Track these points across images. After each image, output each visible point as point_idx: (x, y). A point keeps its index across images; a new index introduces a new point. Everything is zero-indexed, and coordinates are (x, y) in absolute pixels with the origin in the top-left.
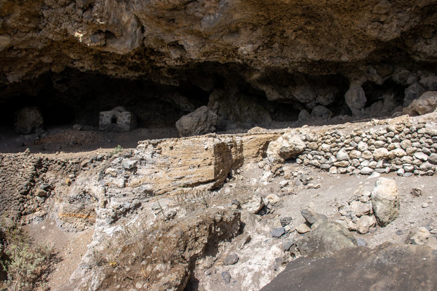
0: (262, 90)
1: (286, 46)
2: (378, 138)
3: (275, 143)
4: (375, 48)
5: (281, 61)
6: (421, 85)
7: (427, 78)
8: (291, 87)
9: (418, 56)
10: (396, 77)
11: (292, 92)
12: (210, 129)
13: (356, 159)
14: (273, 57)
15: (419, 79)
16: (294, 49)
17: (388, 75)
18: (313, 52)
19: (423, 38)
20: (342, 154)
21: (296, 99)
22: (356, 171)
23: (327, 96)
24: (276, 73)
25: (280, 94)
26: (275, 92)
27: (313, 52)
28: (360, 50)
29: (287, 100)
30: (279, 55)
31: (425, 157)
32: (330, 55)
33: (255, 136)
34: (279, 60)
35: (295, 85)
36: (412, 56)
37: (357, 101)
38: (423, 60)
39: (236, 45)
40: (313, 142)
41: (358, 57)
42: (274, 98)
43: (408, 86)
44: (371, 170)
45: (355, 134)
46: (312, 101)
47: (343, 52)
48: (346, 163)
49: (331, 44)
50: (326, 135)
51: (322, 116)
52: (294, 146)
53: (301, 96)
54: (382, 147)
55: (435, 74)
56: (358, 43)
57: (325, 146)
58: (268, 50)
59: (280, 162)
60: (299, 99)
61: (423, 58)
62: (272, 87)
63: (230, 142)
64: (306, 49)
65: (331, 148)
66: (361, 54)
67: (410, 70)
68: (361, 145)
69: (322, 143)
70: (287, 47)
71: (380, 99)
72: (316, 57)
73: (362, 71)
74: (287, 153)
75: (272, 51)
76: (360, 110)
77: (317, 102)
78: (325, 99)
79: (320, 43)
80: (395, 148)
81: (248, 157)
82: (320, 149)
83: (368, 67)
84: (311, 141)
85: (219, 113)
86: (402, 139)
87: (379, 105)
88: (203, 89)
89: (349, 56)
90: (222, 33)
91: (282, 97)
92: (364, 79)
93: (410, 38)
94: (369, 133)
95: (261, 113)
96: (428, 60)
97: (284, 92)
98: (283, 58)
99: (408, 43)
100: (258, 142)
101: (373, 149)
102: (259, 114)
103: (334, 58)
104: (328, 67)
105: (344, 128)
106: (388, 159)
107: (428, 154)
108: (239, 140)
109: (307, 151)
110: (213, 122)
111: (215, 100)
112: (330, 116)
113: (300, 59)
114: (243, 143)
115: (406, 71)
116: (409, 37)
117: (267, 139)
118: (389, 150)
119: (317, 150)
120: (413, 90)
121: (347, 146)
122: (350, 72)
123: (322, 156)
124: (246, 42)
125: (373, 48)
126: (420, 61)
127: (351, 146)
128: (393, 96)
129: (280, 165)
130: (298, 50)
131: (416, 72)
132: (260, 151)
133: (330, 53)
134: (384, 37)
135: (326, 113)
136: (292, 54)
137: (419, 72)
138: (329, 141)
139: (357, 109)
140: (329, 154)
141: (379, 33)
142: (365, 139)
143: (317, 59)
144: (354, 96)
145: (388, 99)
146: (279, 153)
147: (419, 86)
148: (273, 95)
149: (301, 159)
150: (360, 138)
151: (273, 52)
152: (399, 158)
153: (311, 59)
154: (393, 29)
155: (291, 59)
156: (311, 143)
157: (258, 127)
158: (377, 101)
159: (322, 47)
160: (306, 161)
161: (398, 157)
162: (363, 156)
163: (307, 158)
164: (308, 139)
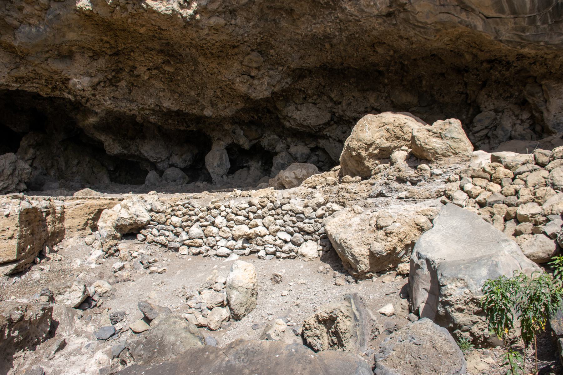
0: (99, 140)
1: (136, 86)
2: (239, 212)
3: (110, 212)
4: (244, 105)
5: (128, 105)
6: (290, 154)
7: (296, 147)
8: (138, 140)
9: (289, 121)
10: (265, 143)
11: (140, 146)
12: (19, 187)
13: (212, 238)
14: (117, 99)
15: (288, 147)
16: (146, 92)
17: (256, 139)
18: (170, 99)
19: (294, 102)
20: (195, 230)
21: (144, 156)
22: (212, 252)
23: (184, 157)
24: (120, 119)
25: (123, 148)
26: (117, 145)
27: (170, 99)
28: (227, 104)
29: (132, 156)
30: (126, 96)
31: (288, 238)
32: (191, 106)
33: (83, 200)
34: (125, 103)
35: (144, 138)
36: (282, 121)
37: (219, 166)
38: (293, 127)
39: (66, 75)
40: (160, 214)
41: (223, 114)
42: (115, 153)
43: (276, 154)
44: (228, 251)
45: (213, 206)
46: (164, 160)
47: (206, 105)
48: (200, 241)
49: (193, 93)
50: (177, 205)
51: (175, 181)
52: (135, 217)
53: (151, 153)
54: (242, 223)
55: (304, 144)
56: (225, 96)
57: (175, 219)
58: (112, 89)
59: (115, 237)
60: (148, 157)
62: (113, 137)
63: (46, 207)
64: (161, 94)
65: (183, 222)
66: (228, 110)
67: (280, 136)
68: (219, 220)
69: (172, 216)
70: (137, 88)
71: (246, 167)
72: (173, 106)
73: (227, 130)
74: (126, 226)
75: (117, 90)
76: (222, 177)
77: (170, 163)
78: (181, 160)
79: (179, 89)
80: (257, 226)
81: (71, 230)
82: (168, 223)
83: (234, 127)
84: (158, 212)
85: (34, 165)
86: (265, 215)
87: (244, 172)
88: (13, 129)
89: (213, 110)
90: (47, 55)
91: (125, 152)
92: (228, 141)
93: (281, 100)
94: (229, 206)
95: (95, 170)
96: (298, 128)
97: (129, 145)
98: (132, 101)
99: (279, 105)
100: (87, 210)
101: (232, 225)
102: (93, 172)
103: (195, 111)
104: (187, 120)
105: (200, 198)
106: (248, 239)
107: (291, 234)
108: (60, 205)
109: (152, 224)
110: (23, 177)
111: (30, 146)
112: (186, 182)
113: (153, 106)
114: (65, 210)
115: (276, 137)
116: (280, 99)
117: (100, 206)
118: (250, 228)
119: (164, 223)
120: (282, 159)
121: (202, 220)
122: (213, 130)
123: (171, 232)
124: (81, 73)
125: (241, 105)
126: (291, 127)
127: (206, 220)
128: (260, 164)
129: (115, 241)
130: (151, 93)
131: (286, 139)
132: (89, 222)
133: (191, 104)
134: (254, 95)
135: (180, 178)
136: (143, 98)
137: (289, 140)
138: (180, 213)
139: (218, 175)
140: (179, 230)
141: (249, 89)
142: (224, 213)
143: (175, 108)
144: (216, 160)
145: (255, 166)
146: (115, 225)
147: (288, 155)
148: (113, 147)
149: (144, 235)
150: (217, 212)
151: (118, 92)
152: (260, 238)
153: (166, 108)
154: (264, 87)
155: (142, 104)
156: (157, 215)
157: (89, 189)
158: (242, 168)
159: (181, 94)
160: (150, 238)
161: (259, 236)
162: (221, 233)
163: (151, 234)
164: (154, 209)
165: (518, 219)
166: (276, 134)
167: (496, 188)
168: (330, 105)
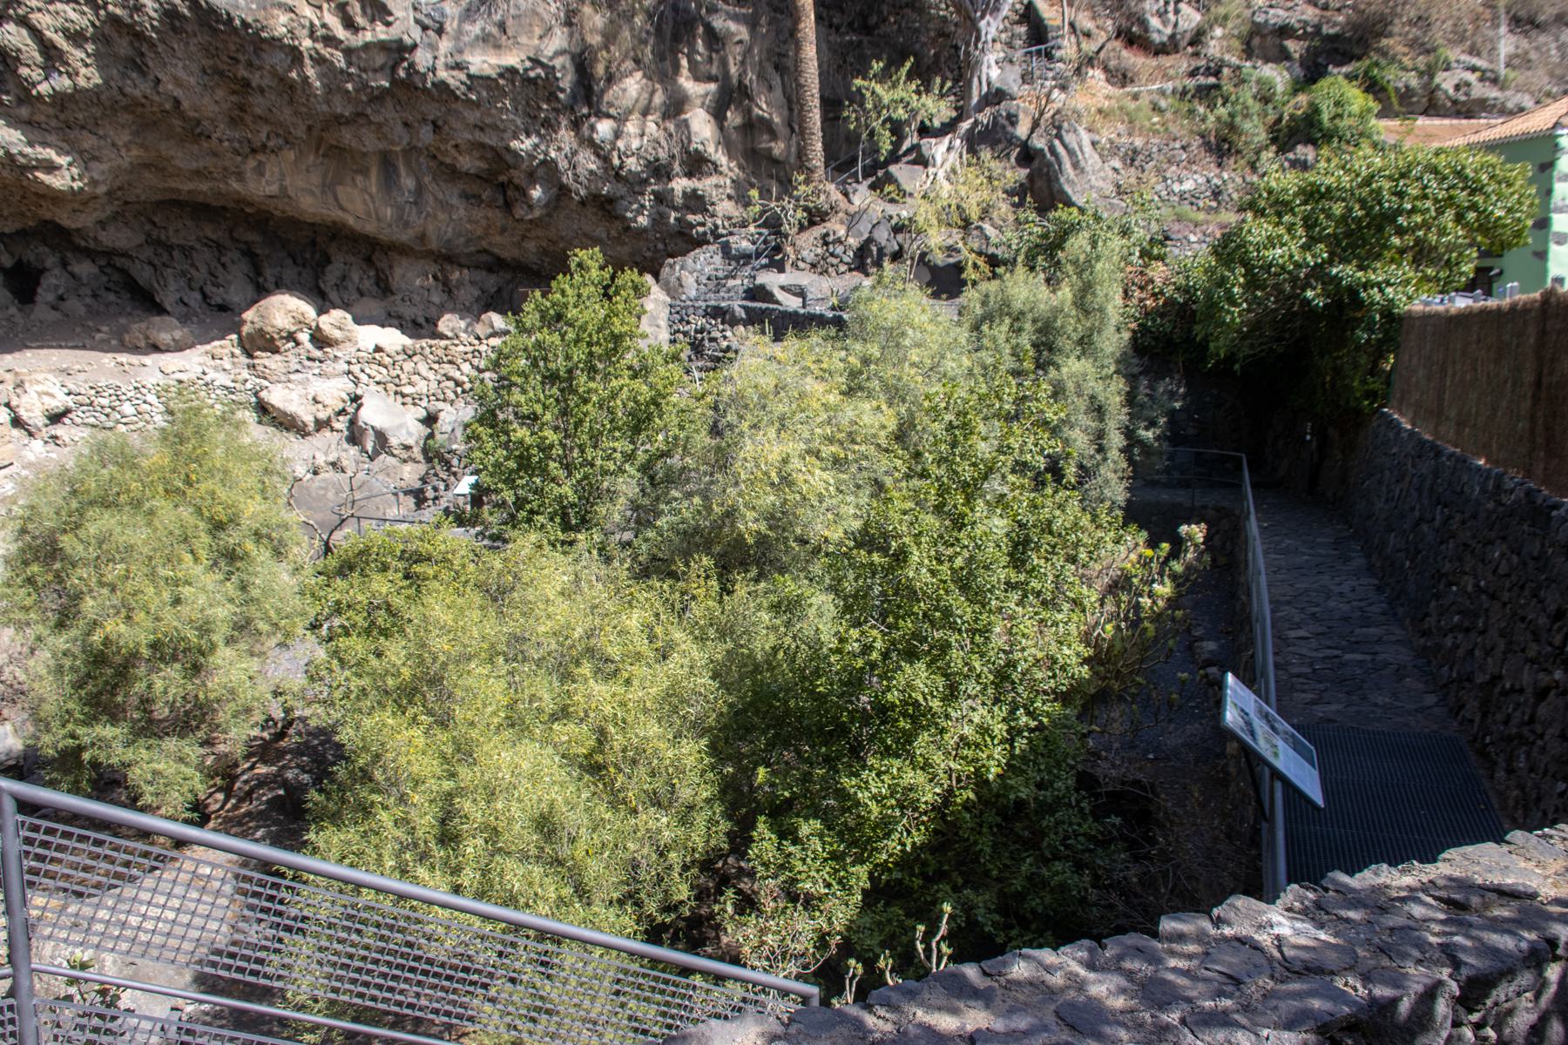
6: (73, 275)
10: (29, 256)
15: (64, 264)
43: (42, 271)
61: (92, 245)
67: (52, 247)
68: (151, 398)
137: (69, 255)
140: (108, 410)
165: (404, 396)
166: (46, 244)
167: (384, 371)
168: (148, 227)
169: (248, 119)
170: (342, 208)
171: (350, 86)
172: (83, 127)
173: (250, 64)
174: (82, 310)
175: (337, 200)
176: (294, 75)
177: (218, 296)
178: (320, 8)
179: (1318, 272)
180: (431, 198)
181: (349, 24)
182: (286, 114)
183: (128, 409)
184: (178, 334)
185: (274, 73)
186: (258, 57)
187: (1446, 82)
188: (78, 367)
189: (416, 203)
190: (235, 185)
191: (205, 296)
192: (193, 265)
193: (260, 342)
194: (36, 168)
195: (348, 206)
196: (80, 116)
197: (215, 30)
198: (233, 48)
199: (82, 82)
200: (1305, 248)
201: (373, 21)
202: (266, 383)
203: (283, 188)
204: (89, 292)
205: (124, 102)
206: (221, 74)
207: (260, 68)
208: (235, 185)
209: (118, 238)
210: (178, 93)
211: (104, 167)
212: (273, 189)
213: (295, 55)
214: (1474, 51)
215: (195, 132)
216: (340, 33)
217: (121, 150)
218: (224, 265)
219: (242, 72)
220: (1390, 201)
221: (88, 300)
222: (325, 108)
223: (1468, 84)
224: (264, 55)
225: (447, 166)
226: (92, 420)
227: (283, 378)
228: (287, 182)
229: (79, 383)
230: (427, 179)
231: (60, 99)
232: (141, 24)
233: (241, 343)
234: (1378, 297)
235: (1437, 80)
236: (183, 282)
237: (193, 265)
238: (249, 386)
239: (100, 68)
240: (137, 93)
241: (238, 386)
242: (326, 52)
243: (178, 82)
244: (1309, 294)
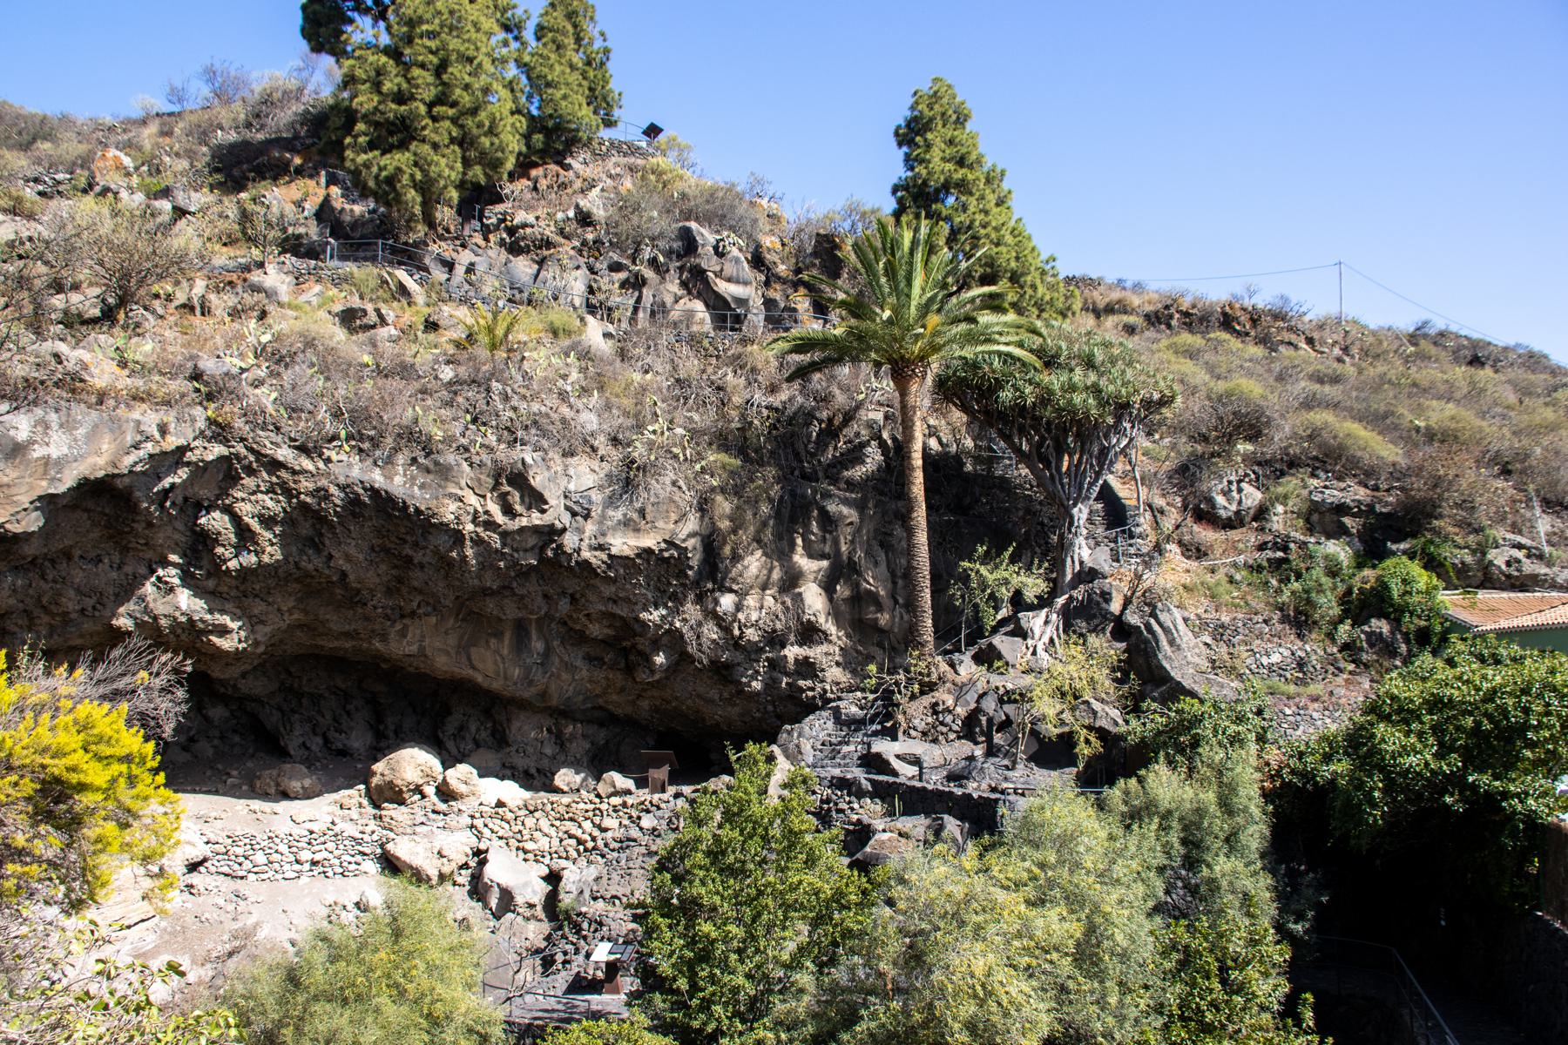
20: (260, 858)
22: (279, 876)
68: (283, 848)
165: (526, 852)
167: (506, 826)
169: (404, 590)
170: (474, 668)
171: (502, 564)
172: (256, 596)
173: (416, 545)
174: (210, 752)
175: (469, 659)
176: (454, 554)
177: (339, 741)
178: (484, 497)
179: (1456, 781)
180: (557, 660)
181: (508, 511)
182: (440, 587)
183: (260, 858)
184: (307, 782)
185: (436, 552)
186: (425, 539)
187: (1498, 558)
188: (214, 814)
189: (542, 664)
190: (378, 645)
191: (326, 741)
192: (319, 712)
193: (388, 794)
194: (211, 632)
195: (480, 666)
196: (257, 587)
197: (390, 516)
198: (403, 530)
199: (266, 559)
200: (1439, 756)
201: (529, 508)
202: (392, 835)
203: (422, 649)
204: (217, 734)
205: (298, 574)
206: (387, 551)
207: (424, 548)
208: (378, 645)
209: (257, 686)
210: (347, 567)
211: (268, 629)
212: (414, 649)
213: (458, 537)
214: (1515, 529)
215: (353, 599)
216: (499, 518)
217: (284, 613)
218: (348, 713)
219: (408, 551)
220: (1515, 717)
221: (216, 742)
222: (476, 582)
223: (1518, 561)
224: (430, 537)
225: (576, 632)
226: (226, 869)
227: (409, 830)
228: (426, 643)
229: (216, 831)
230: (555, 643)
231: (244, 572)
232: (326, 510)
233: (369, 794)
234: (1519, 808)
235: (1489, 557)
236: (307, 727)
237: (319, 712)
238: (375, 837)
239: (283, 547)
240: (310, 567)
241: (366, 837)
242: (485, 535)
243: (348, 558)
244: (1448, 800)
